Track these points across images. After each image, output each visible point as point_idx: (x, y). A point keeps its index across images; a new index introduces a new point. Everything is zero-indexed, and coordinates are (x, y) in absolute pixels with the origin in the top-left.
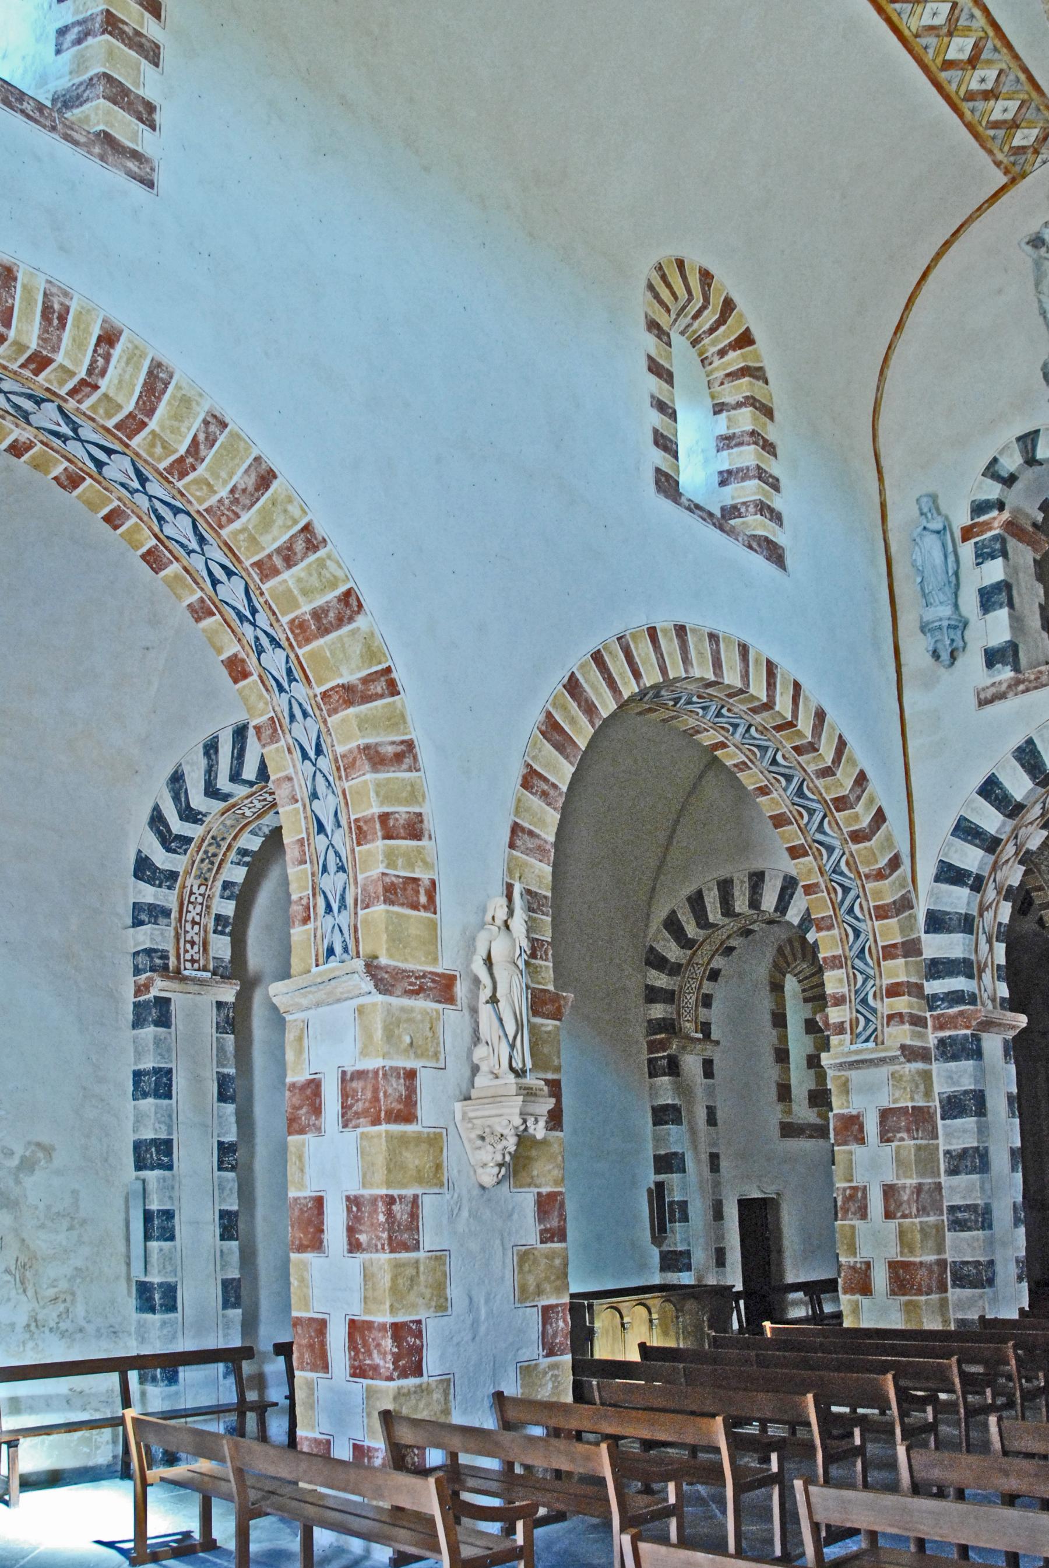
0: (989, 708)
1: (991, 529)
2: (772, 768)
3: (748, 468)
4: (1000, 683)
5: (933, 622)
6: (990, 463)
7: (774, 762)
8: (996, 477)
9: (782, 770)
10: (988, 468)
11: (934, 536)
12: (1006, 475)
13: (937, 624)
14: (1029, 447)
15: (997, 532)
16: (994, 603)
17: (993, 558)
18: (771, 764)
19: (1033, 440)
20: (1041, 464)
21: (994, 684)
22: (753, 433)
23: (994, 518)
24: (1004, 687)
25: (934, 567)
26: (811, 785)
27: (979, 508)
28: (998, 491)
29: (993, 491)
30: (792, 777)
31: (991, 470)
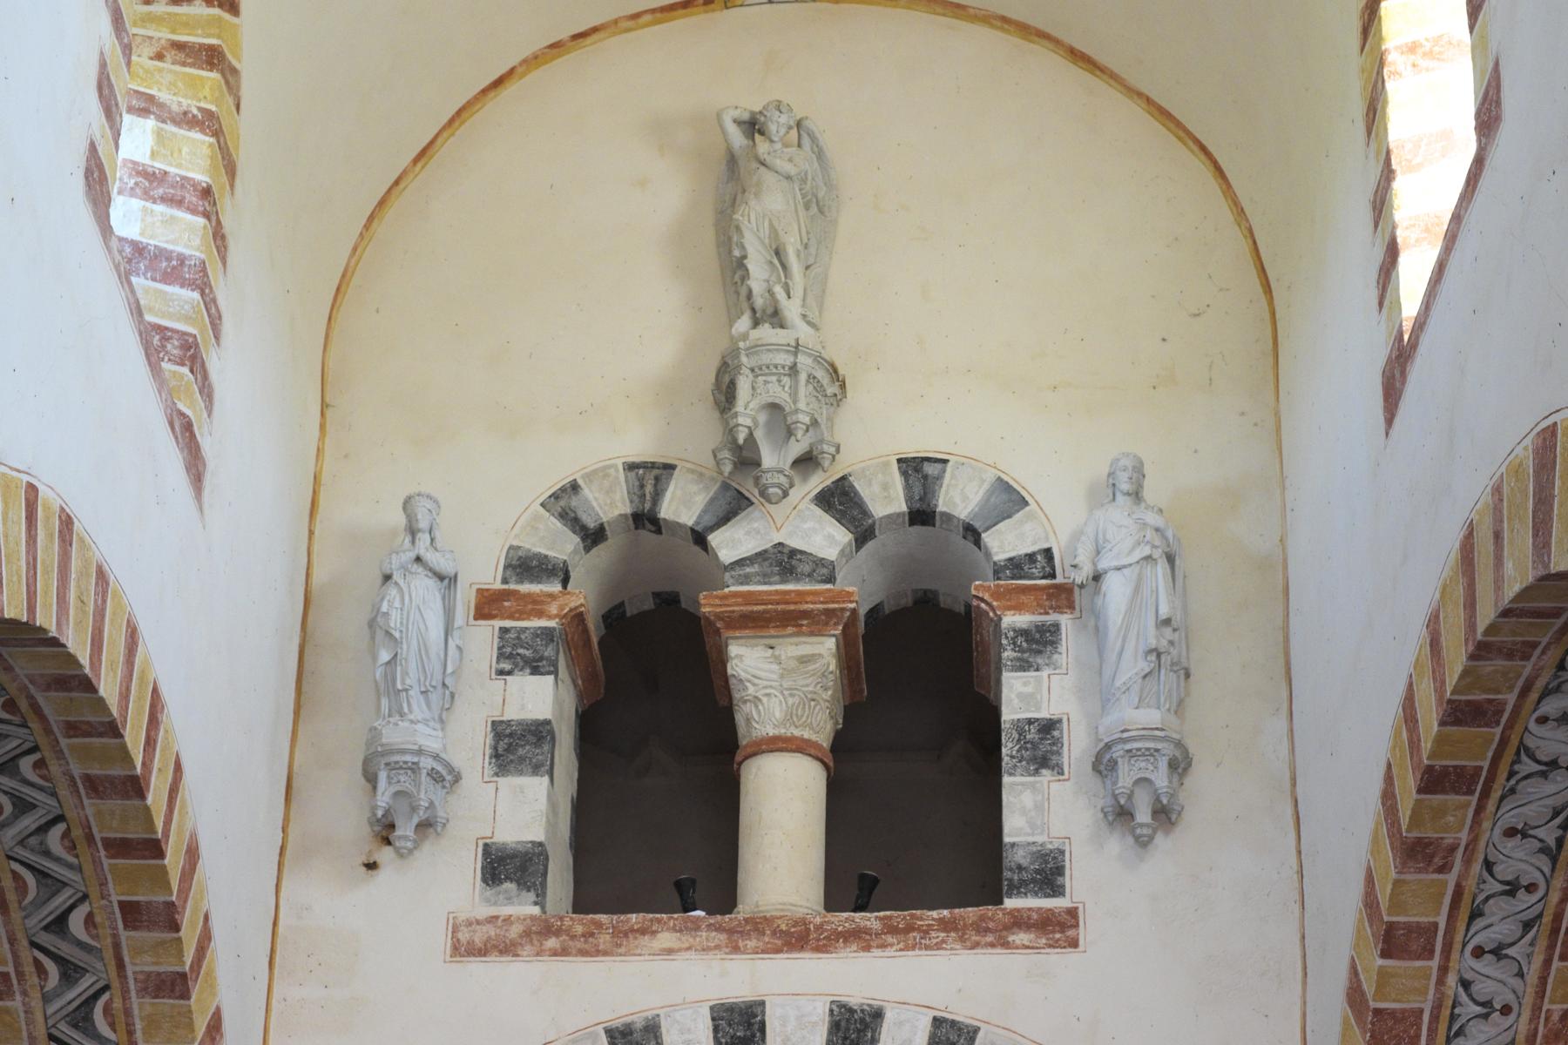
0: (477, 969)
1: (540, 614)
2: (46, 939)
3: (182, 259)
4: (508, 920)
5: (403, 752)
6: (563, 490)
7: (59, 924)
8: (571, 520)
9: (65, 949)
10: (555, 496)
11: (432, 583)
12: (592, 525)
13: (408, 758)
14: (649, 489)
15: (552, 624)
16: (522, 759)
17: (536, 671)
18: (46, 928)
19: (657, 479)
20: (659, 531)
21: (493, 919)
22: (207, 192)
23: (552, 596)
24: (515, 931)
25: (424, 647)
26: (117, 1004)
27: (525, 566)
28: (570, 548)
29: (561, 545)
30: (81, 971)
31: (562, 503)
